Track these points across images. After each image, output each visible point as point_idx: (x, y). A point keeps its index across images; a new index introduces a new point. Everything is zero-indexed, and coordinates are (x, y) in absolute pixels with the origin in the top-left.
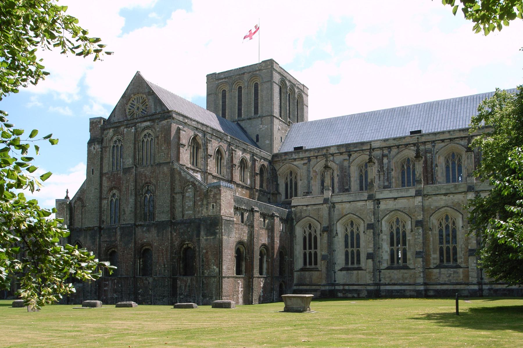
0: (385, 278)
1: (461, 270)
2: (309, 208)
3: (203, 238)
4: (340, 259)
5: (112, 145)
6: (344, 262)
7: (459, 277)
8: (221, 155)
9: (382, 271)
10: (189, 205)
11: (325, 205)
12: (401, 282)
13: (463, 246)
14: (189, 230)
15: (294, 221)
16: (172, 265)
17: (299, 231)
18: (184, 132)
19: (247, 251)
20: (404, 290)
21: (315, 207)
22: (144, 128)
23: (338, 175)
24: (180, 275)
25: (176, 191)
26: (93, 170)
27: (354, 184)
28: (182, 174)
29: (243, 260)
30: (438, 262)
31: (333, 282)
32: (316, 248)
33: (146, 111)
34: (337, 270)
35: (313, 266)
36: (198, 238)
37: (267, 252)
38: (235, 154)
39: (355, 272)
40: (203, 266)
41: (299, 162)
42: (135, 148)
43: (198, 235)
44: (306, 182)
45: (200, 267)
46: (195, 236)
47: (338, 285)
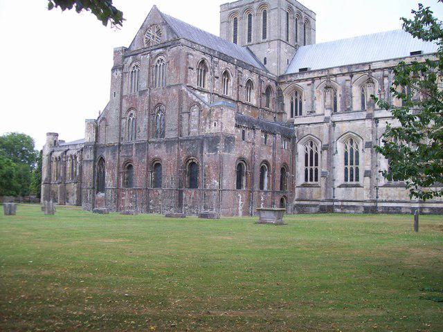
4: (339, 176)
6: (343, 179)
11: (325, 124)
17: (301, 149)
18: (192, 57)
20: (400, 208)
21: (316, 126)
25: (184, 110)
27: (356, 105)
31: (332, 198)
32: (316, 164)
35: (314, 182)
40: (205, 179)
41: (303, 83)
43: (202, 152)
44: (310, 102)
47: (337, 201)
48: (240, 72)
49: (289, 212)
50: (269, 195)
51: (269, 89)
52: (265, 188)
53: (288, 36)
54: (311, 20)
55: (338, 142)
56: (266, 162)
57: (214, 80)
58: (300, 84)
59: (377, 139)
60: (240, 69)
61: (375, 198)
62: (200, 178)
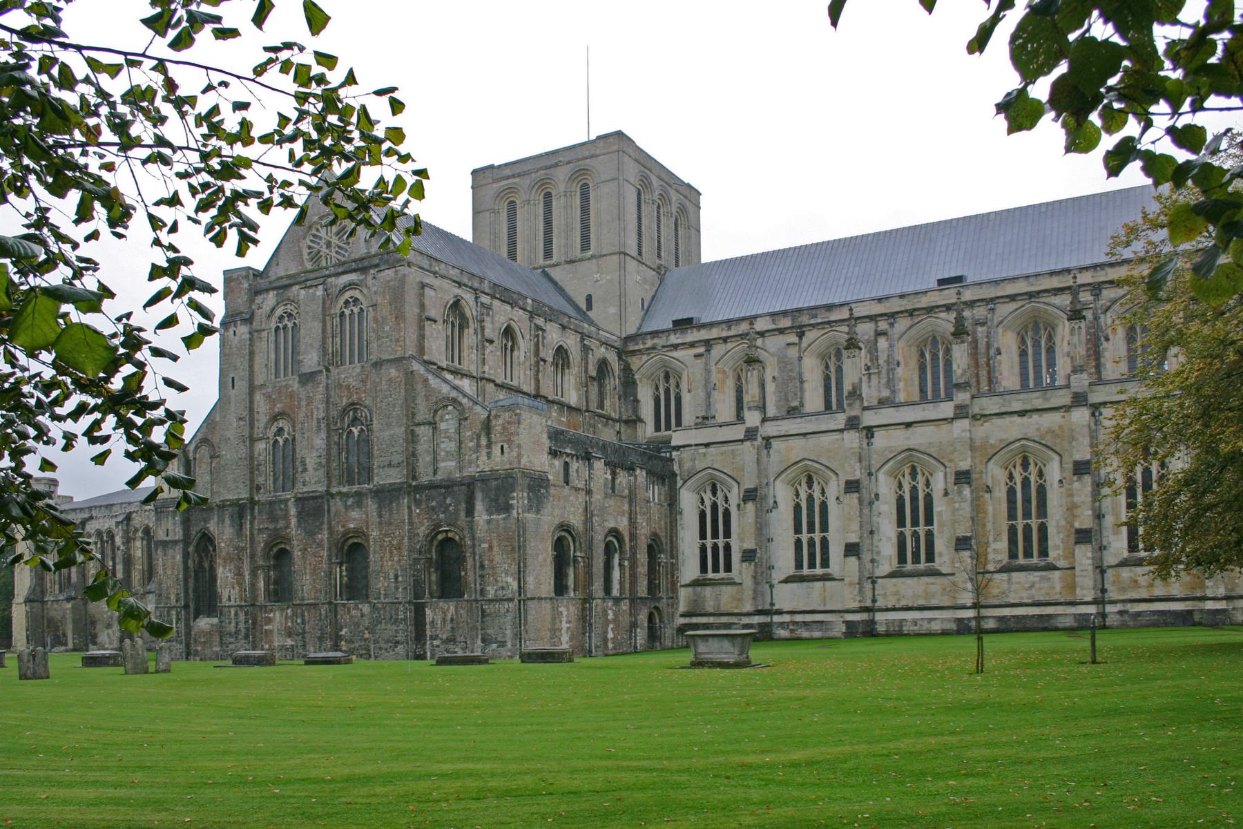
0: (885, 595)
1: (1057, 574)
2: (712, 449)
3: (481, 515)
4: (783, 559)
5: (273, 325)
6: (792, 563)
7: (1052, 588)
8: (513, 339)
9: (879, 581)
10: (448, 449)
12: (921, 602)
13: (1063, 523)
14: (448, 501)
15: (678, 478)
16: (414, 576)
17: (688, 501)
19: (577, 544)
21: (724, 448)
22: (344, 287)
23: (774, 378)
24: (432, 597)
25: (419, 418)
26: (233, 378)
29: (568, 564)
30: (1004, 558)
31: (767, 607)
32: (727, 534)
33: (346, 251)
34: (775, 582)
35: (722, 574)
36: (469, 519)
37: (620, 547)
38: (544, 338)
39: (818, 584)
40: (482, 576)
42: (324, 331)
43: (470, 512)
44: (703, 395)
45: (475, 580)
46: (462, 514)
47: (779, 612)
48: (538, 328)
49: (668, 643)
50: (625, 606)
51: (603, 365)
52: (615, 592)
53: (640, 246)
54: (690, 208)
55: (778, 482)
56: (615, 532)
57: (484, 348)
58: (675, 354)
59: (870, 474)
60: (540, 321)
61: (868, 603)
62: (470, 575)
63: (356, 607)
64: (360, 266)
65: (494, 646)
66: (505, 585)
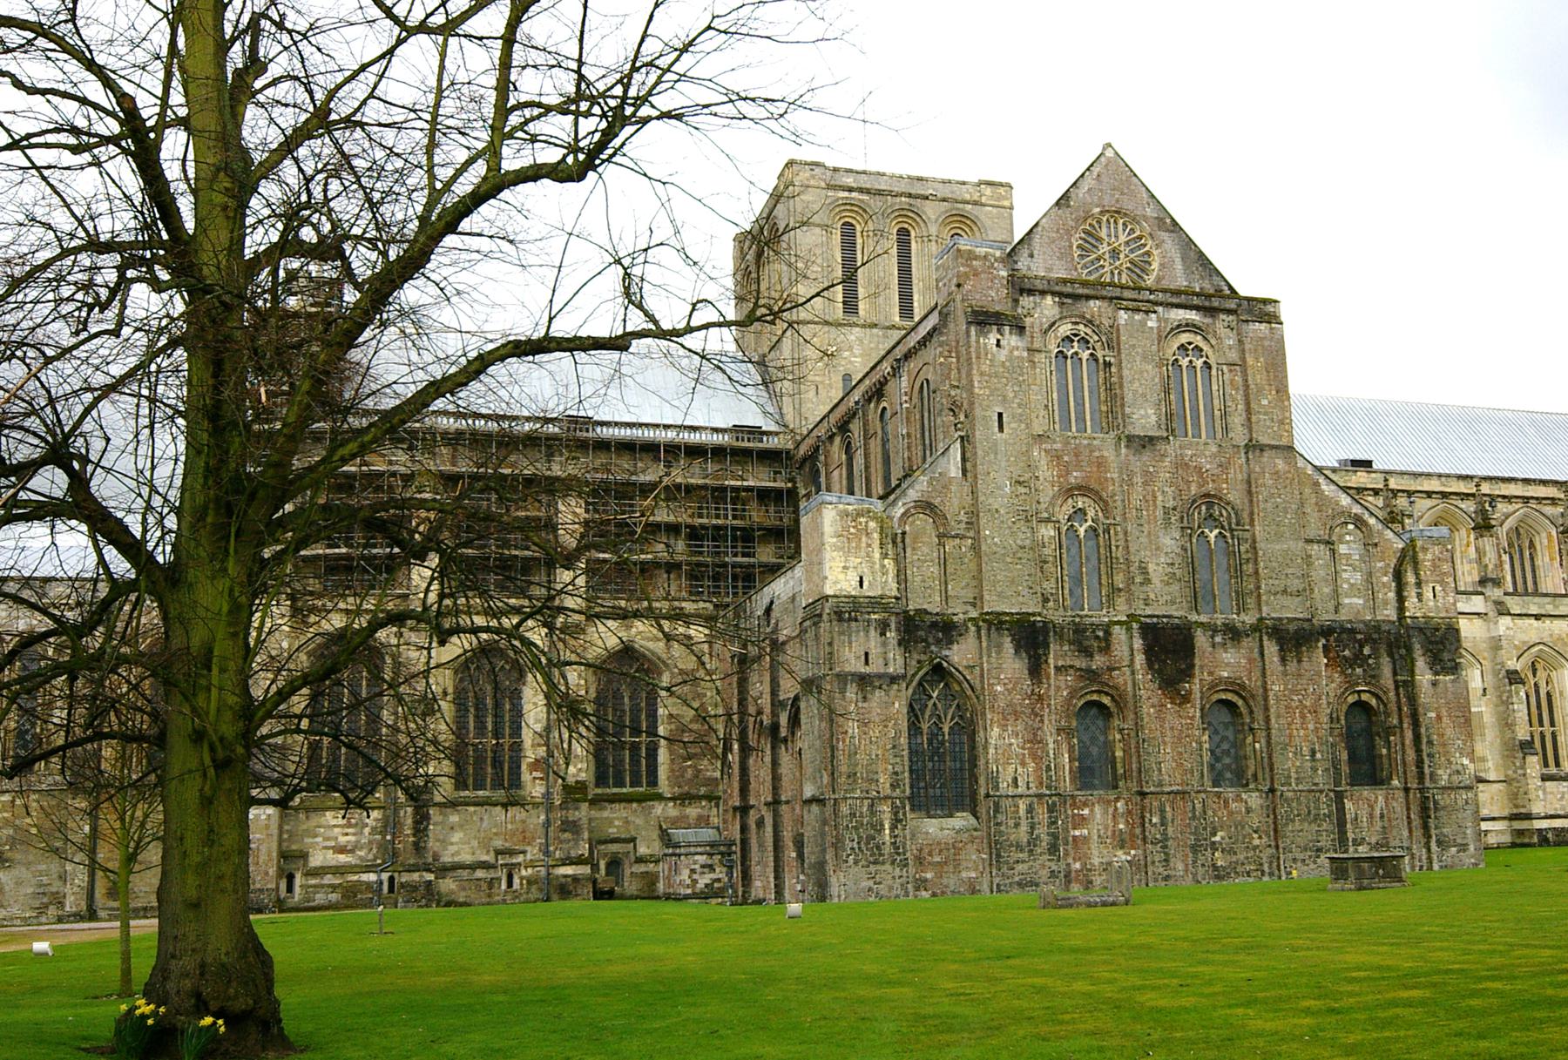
28: (1324, 487)
63: (1238, 798)
64: (1207, 304)
65: (1454, 850)
66: (1460, 768)
